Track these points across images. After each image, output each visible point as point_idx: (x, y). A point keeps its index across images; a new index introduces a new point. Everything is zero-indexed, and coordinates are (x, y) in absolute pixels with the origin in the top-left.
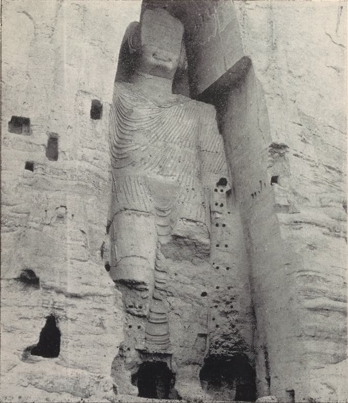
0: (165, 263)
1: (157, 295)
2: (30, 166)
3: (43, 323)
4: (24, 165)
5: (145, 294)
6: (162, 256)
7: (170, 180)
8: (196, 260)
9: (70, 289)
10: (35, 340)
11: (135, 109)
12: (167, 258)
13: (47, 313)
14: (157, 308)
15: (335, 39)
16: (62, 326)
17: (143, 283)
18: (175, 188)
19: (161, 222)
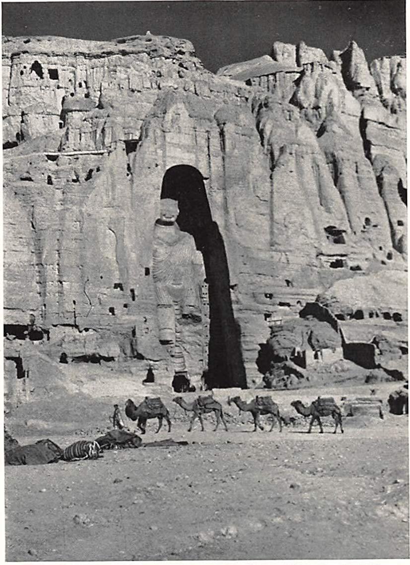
0: (179, 327)
1: (178, 344)
2: (125, 306)
3: (147, 372)
4: (123, 306)
5: (172, 345)
6: (178, 325)
7: (179, 287)
8: (195, 324)
9: (155, 359)
10: (145, 378)
11: (158, 250)
12: (180, 325)
13: (148, 368)
14: (177, 350)
15: (261, 198)
16: (153, 371)
17: (171, 341)
18: (183, 290)
19: (177, 307)
